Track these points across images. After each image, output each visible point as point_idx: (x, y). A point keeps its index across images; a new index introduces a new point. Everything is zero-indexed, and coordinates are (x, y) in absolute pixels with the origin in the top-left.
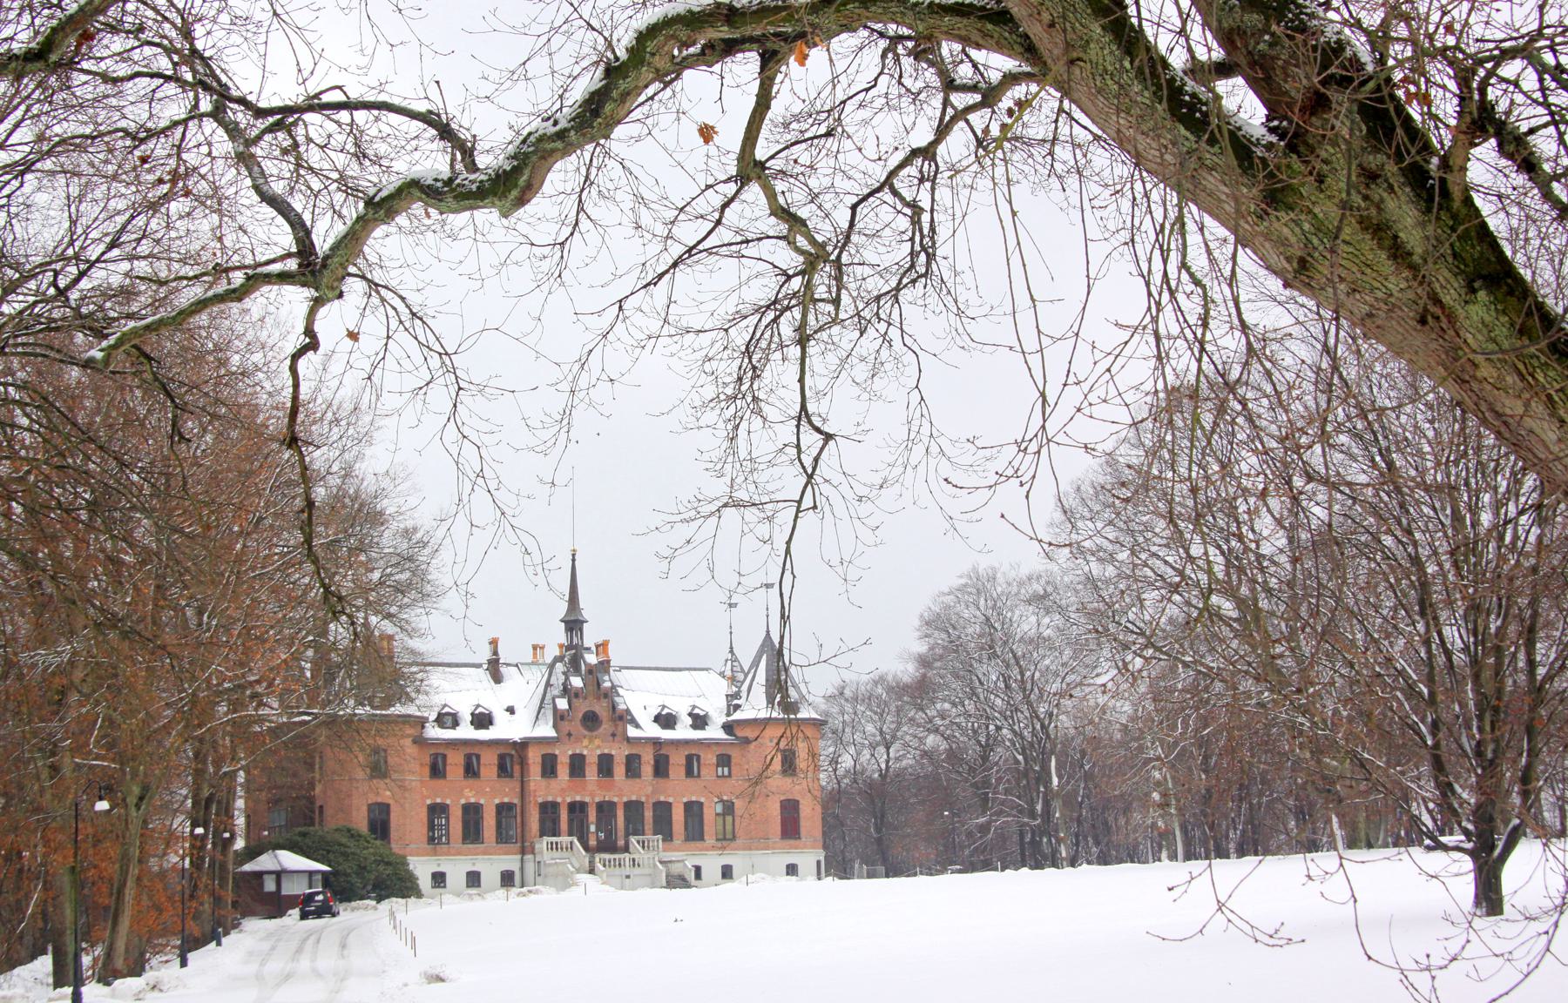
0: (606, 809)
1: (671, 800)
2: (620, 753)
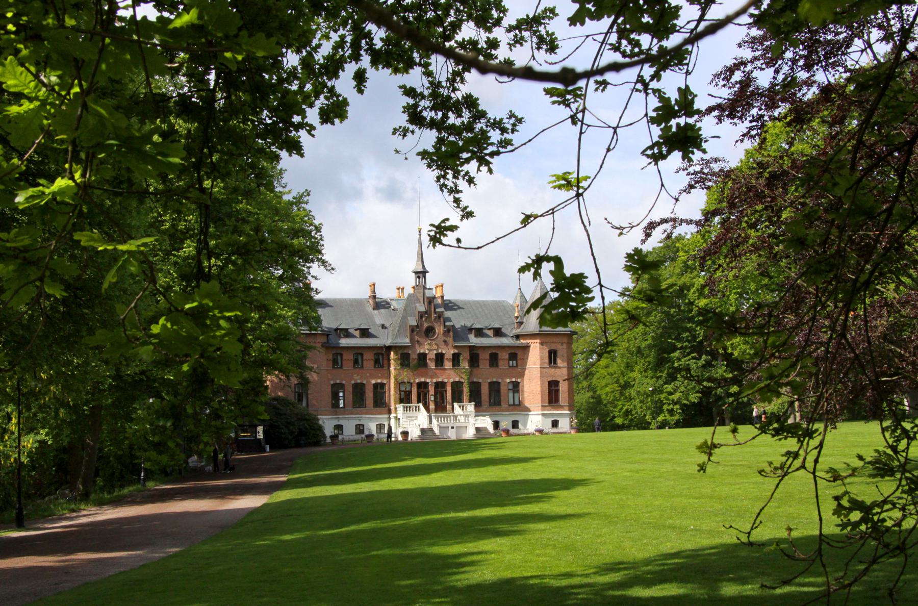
0: (440, 386)
1: (480, 381)
2: (449, 352)
